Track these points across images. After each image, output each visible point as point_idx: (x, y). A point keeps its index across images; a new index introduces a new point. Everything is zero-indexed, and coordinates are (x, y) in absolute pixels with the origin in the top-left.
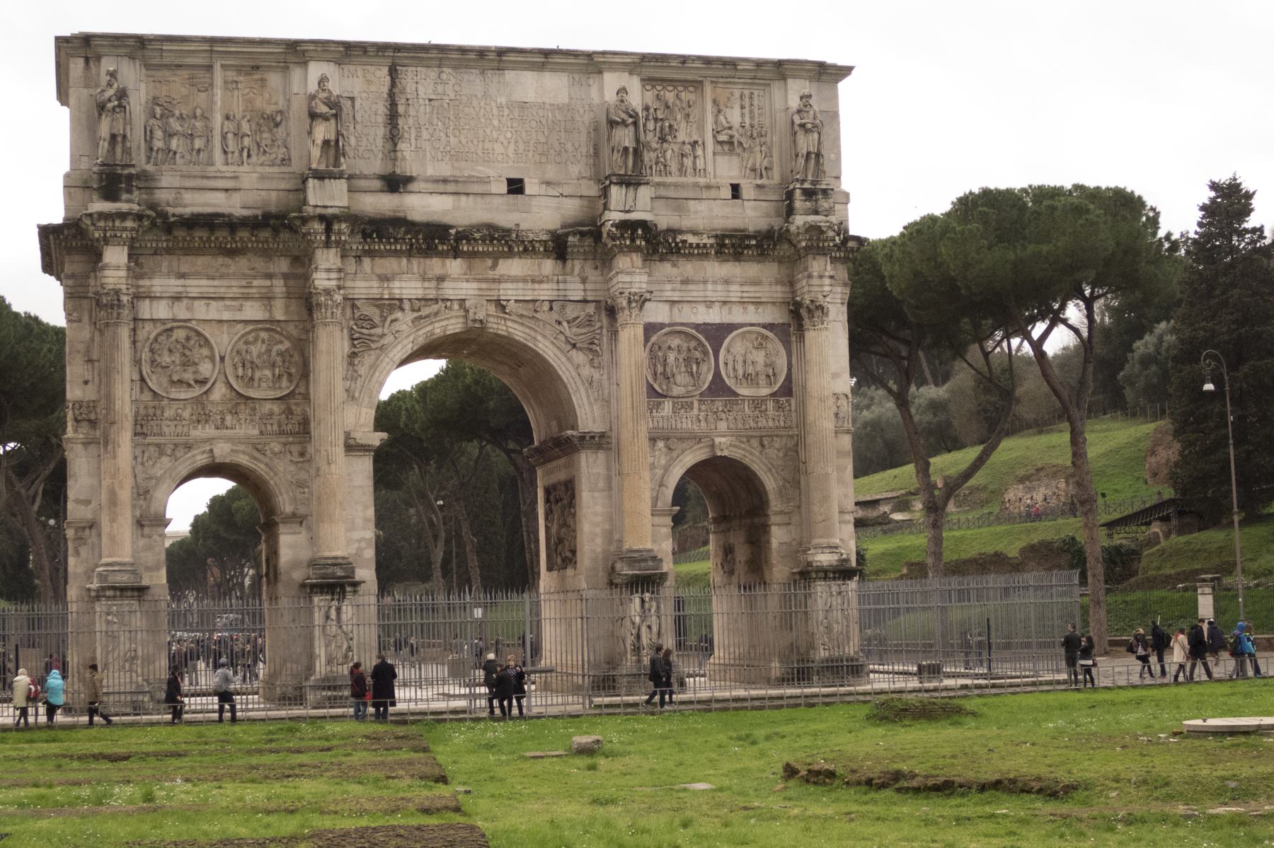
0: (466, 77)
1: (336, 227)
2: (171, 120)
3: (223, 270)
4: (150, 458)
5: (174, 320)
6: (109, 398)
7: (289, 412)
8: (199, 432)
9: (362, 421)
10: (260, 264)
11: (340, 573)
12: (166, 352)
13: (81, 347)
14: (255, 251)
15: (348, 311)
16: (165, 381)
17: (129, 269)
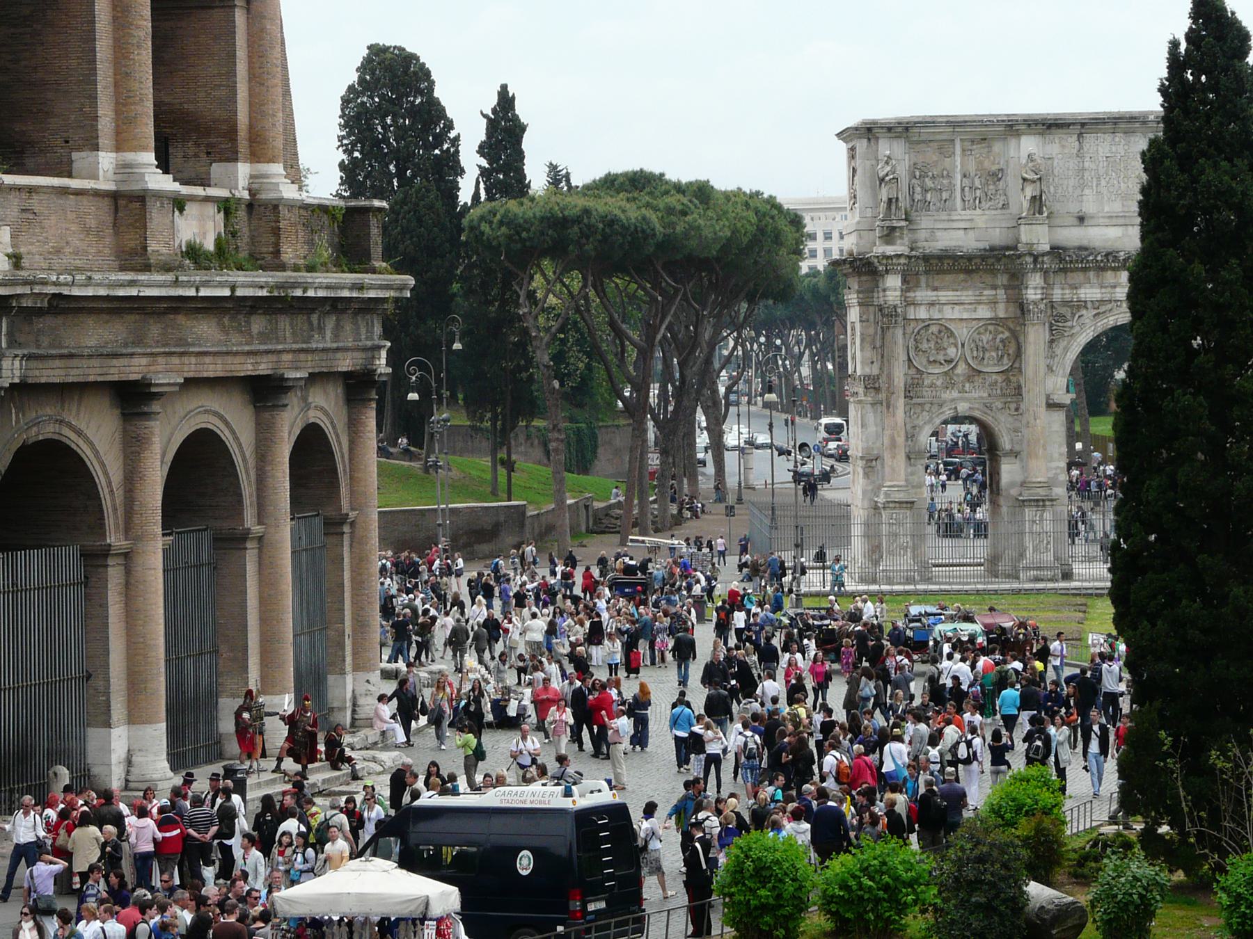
0: (1132, 139)
1: (1040, 259)
2: (927, 180)
3: (963, 284)
4: (915, 413)
5: (930, 319)
6: (890, 377)
7: (1008, 381)
8: (947, 395)
9: (1058, 386)
10: (988, 279)
11: (1042, 492)
12: (925, 341)
13: (868, 339)
14: (985, 271)
15: (1049, 311)
16: (924, 362)
17: (902, 291)
